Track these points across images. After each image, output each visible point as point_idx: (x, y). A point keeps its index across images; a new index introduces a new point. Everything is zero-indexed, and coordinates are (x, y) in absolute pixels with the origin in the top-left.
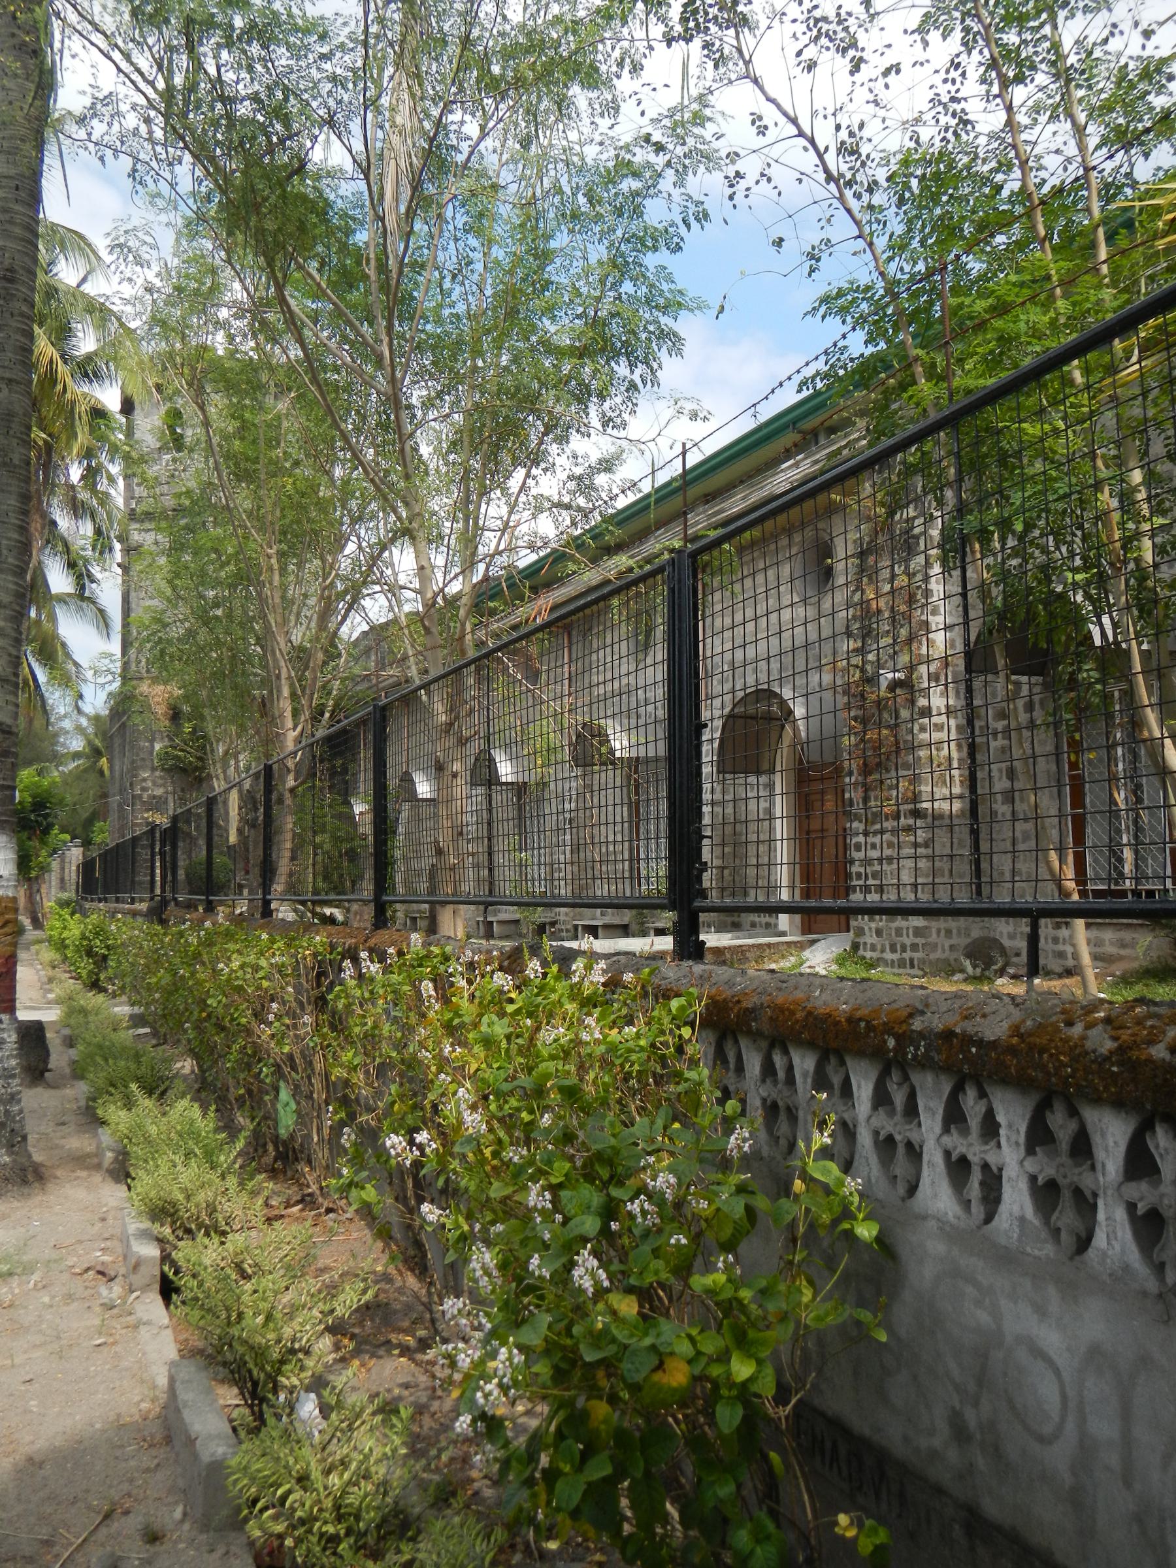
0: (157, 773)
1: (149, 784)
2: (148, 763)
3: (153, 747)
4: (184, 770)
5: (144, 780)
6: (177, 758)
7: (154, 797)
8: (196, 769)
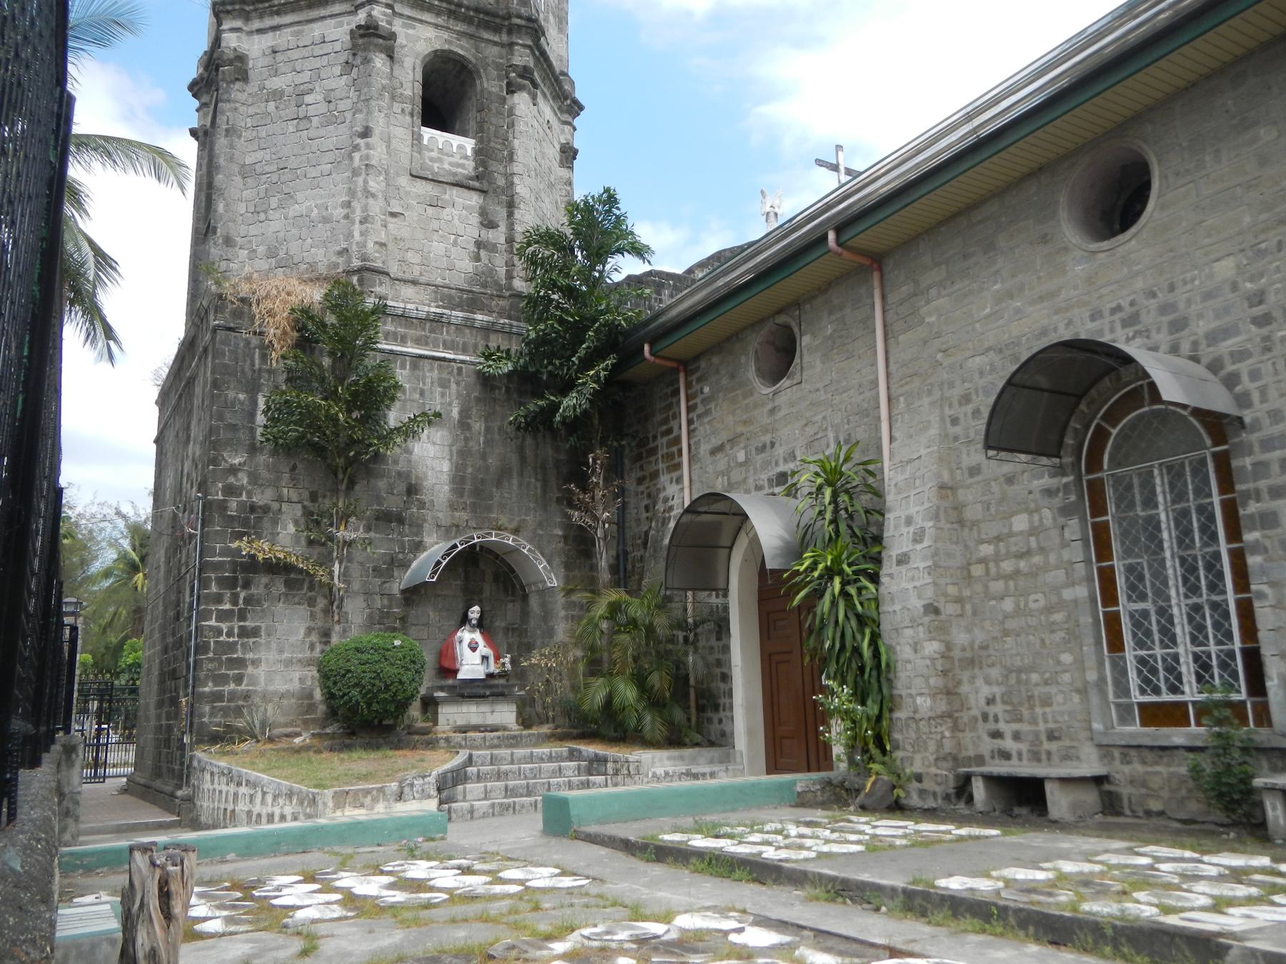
0: (263, 458)
1: (243, 479)
2: (243, 435)
3: (254, 403)
4: (319, 450)
5: (233, 470)
6: (309, 413)
7: (253, 508)
8: (352, 442)
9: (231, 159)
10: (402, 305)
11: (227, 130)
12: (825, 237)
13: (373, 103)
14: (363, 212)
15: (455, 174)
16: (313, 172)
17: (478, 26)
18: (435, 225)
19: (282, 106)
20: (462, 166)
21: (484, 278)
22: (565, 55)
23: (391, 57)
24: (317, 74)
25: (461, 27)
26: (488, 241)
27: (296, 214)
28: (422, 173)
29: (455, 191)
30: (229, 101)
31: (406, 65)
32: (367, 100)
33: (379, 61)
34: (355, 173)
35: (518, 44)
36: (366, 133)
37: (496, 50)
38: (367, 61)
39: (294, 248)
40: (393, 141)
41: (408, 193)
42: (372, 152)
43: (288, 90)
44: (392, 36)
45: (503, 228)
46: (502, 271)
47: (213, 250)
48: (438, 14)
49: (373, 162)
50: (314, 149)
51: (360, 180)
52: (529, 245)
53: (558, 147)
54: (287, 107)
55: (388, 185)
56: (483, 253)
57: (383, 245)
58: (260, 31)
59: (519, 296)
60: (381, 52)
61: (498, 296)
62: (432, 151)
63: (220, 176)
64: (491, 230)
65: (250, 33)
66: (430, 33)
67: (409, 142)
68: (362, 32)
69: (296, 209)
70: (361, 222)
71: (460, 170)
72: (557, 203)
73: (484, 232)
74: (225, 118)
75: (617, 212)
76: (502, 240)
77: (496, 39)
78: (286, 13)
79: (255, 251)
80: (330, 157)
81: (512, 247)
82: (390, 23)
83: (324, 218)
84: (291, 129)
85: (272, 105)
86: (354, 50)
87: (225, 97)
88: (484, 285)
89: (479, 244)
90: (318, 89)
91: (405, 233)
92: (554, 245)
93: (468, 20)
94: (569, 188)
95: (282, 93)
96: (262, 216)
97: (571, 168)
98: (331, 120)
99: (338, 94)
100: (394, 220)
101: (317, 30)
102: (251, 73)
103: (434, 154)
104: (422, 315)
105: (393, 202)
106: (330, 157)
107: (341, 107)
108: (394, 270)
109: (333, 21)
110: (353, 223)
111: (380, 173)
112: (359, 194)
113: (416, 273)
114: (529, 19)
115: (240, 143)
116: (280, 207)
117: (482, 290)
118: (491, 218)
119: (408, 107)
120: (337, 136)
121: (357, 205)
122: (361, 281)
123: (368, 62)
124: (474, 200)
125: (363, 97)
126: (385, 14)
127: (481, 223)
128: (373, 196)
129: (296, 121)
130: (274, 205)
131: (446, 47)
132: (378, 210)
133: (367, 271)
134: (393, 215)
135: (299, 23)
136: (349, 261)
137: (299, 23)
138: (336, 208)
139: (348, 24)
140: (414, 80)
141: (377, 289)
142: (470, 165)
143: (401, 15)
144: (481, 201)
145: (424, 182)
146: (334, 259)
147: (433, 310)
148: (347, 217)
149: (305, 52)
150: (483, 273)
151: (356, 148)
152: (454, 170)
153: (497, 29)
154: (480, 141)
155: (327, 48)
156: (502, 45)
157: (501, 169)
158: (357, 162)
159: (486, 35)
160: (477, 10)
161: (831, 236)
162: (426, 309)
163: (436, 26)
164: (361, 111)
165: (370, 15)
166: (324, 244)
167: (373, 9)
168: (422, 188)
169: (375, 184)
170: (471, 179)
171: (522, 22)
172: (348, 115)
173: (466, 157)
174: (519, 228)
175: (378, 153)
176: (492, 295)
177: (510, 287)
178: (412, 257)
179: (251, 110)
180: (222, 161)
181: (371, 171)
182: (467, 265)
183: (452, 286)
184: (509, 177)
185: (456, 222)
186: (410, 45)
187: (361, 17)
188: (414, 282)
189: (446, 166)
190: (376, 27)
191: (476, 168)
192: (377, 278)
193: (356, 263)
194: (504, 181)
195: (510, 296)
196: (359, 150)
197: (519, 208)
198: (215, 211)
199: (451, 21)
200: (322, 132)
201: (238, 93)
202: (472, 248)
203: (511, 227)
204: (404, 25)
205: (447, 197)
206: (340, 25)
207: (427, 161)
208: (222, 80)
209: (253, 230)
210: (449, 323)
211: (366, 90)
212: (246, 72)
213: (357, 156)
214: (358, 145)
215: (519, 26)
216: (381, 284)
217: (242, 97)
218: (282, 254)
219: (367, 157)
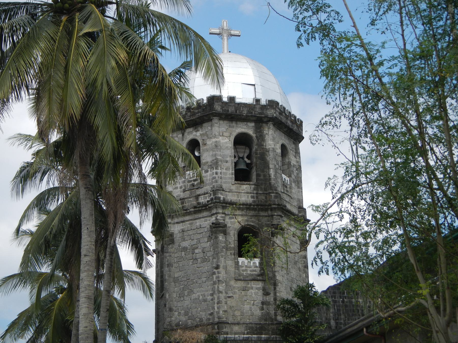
9: (170, 276)
10: (233, 336)
11: (168, 265)
12: (363, 330)
13: (220, 254)
14: (218, 299)
15: (252, 275)
16: (200, 281)
17: (259, 211)
18: (245, 298)
19: (187, 254)
20: (255, 271)
21: (266, 317)
22: (300, 198)
23: (225, 234)
24: (199, 241)
25: (252, 213)
26: (266, 301)
27: (194, 298)
28: (239, 278)
29: (252, 282)
30: (167, 252)
31: (231, 234)
32: (217, 254)
33: (221, 237)
34: (214, 283)
35: (275, 215)
36: (217, 267)
37: (266, 218)
38: (216, 238)
39: (194, 311)
40: (228, 267)
41: (234, 287)
42: (220, 275)
43: (189, 247)
44: (225, 226)
45: (272, 295)
46: (272, 312)
47: (165, 313)
48: (242, 209)
49: (221, 279)
50: (199, 272)
51: (216, 286)
52: (281, 304)
53: (298, 242)
54: (189, 254)
55: (226, 285)
56: (264, 306)
57: (225, 311)
58: (178, 223)
59: (280, 323)
60: (221, 233)
61: (271, 324)
62: (243, 267)
63: (166, 283)
64: (267, 296)
65: (174, 223)
66: (240, 219)
67: (234, 266)
68: (214, 225)
69: (194, 296)
70: (217, 304)
71: (254, 273)
72: (299, 268)
73: (264, 298)
74: (167, 260)
75: (314, 290)
76: (272, 299)
77: (266, 214)
78: (186, 216)
79: (180, 313)
80: (205, 275)
81: (276, 302)
82: (224, 220)
83: (204, 299)
84: (191, 263)
85: (183, 253)
86: (212, 232)
87: (166, 251)
88: (266, 320)
89: (263, 303)
90: (200, 247)
91: (234, 304)
92: (290, 304)
93: (254, 209)
94: (305, 260)
95: (187, 248)
96: (182, 299)
97: (306, 250)
98: (204, 260)
99: (206, 249)
100: (229, 299)
101: (198, 223)
102: (175, 239)
103: (244, 268)
104: (241, 338)
105: (229, 292)
106: (205, 275)
107: (208, 255)
108: (230, 320)
109: (203, 219)
110: (214, 303)
111: (223, 282)
112: (216, 292)
113: (239, 319)
114: (278, 205)
115: (173, 269)
116: (188, 295)
117: (265, 323)
118: (267, 291)
119: (233, 252)
120: (207, 267)
121: (215, 296)
122: (218, 328)
123: (217, 238)
124: (260, 285)
125: (216, 253)
126: (222, 217)
127: (264, 294)
128: (221, 292)
129: (192, 260)
130: (186, 294)
131: (246, 223)
132: (223, 298)
133: (221, 324)
134: (229, 297)
135: (191, 220)
136: (214, 318)
137: (191, 220)
138: (208, 296)
139: (209, 220)
140: (234, 240)
141: (224, 330)
142: (258, 269)
143: (228, 215)
144: (263, 285)
145: (240, 282)
146: (209, 317)
147: (245, 336)
148: (212, 300)
149: (194, 232)
150: (265, 315)
151: (214, 273)
152: (252, 273)
153: (266, 210)
154: (262, 259)
155: (202, 230)
156: (269, 216)
157: (271, 269)
158: (215, 279)
159: (262, 213)
160: (257, 205)
161: (365, 330)
162: (243, 336)
163: (242, 215)
164: (215, 258)
165: (216, 219)
166: (205, 310)
167: (217, 216)
168: (240, 284)
169: (222, 287)
170: (259, 275)
171: (276, 206)
172: (211, 258)
173: (256, 267)
174: (278, 294)
175: (222, 274)
176: (269, 324)
177: (276, 320)
178: (237, 313)
179: (176, 255)
180: (167, 277)
181: (220, 283)
182: (258, 312)
183: (253, 323)
184: (274, 273)
185: (254, 295)
186: (232, 226)
187: (213, 219)
188: (238, 324)
189: (249, 272)
190: (219, 224)
191: (260, 271)
192: (224, 325)
193: (216, 320)
194: (272, 274)
195: (276, 324)
196: (215, 274)
197: (278, 286)
198: (165, 297)
199: (248, 211)
200: (202, 265)
201: (171, 249)
202: (260, 305)
203: (275, 294)
204: (231, 218)
205: (249, 286)
206: (206, 221)
207: (241, 272)
208: (165, 244)
209: (179, 304)
210: (252, 340)
211: (216, 249)
212: (173, 239)
213: (215, 276)
214: (215, 272)
215: (275, 208)
216: (225, 327)
217: (172, 250)
218: (190, 315)
219: (218, 277)
